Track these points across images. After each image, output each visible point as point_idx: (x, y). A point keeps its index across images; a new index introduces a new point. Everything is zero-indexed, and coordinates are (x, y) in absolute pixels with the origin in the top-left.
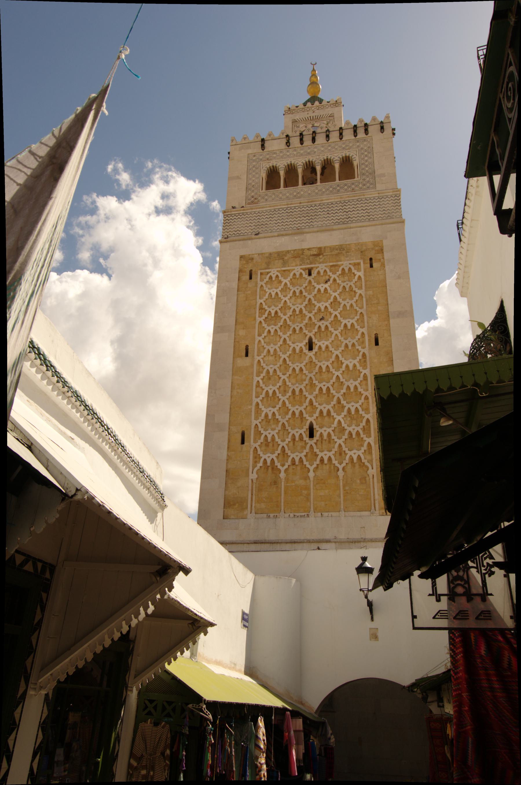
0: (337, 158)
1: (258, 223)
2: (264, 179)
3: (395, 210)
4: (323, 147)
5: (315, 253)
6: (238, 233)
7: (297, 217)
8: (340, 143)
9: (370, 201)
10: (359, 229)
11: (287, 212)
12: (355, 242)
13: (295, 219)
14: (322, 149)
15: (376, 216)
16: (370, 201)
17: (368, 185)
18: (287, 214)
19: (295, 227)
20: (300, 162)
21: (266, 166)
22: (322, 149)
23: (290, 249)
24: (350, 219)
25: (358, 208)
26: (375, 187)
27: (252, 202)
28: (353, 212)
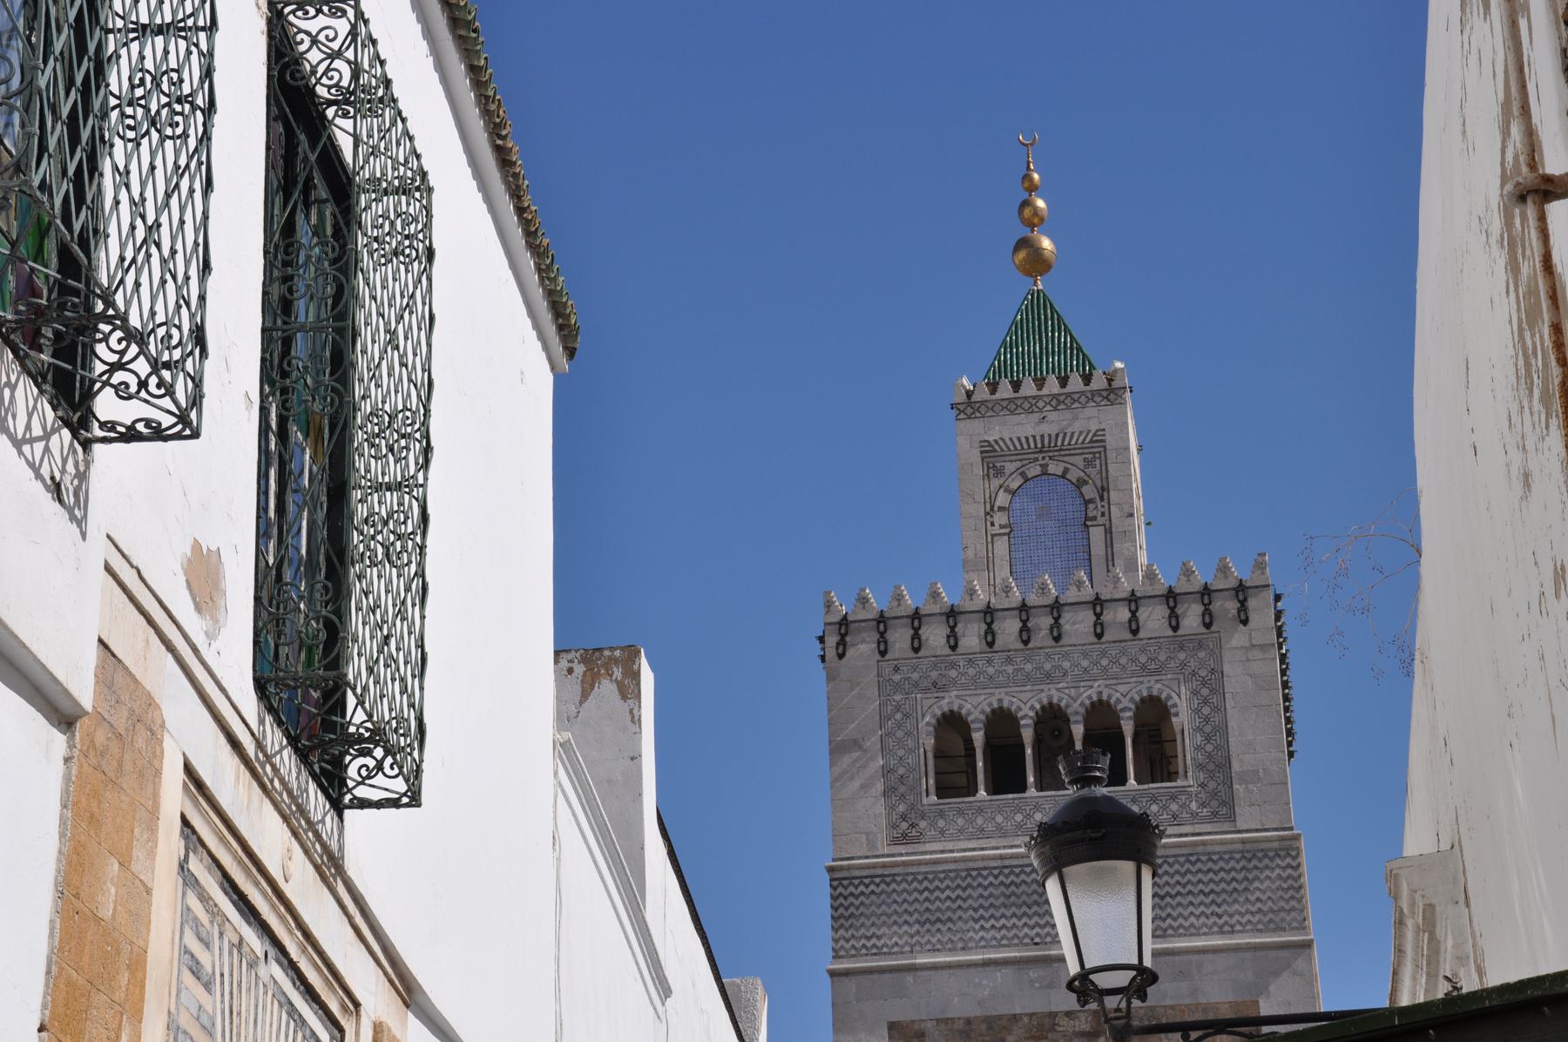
0: (1125, 703)
1: (927, 915)
2: (930, 755)
3: (1287, 901)
4: (1085, 655)
5: (1086, 1027)
6: (874, 946)
7: (1029, 901)
8: (1133, 647)
9: (1221, 864)
10: (1195, 958)
11: (1002, 883)
12: (1187, 1001)
13: (1024, 908)
14: (1085, 663)
15: (1237, 917)
16: (1221, 864)
17: (1214, 804)
18: (1002, 888)
19: (1026, 935)
20: (1026, 706)
21: (930, 710)
22: (1085, 663)
23: (1018, 1011)
24: (1169, 921)
25: (1189, 887)
26: (1231, 817)
27: (904, 835)
28: (1179, 898)
